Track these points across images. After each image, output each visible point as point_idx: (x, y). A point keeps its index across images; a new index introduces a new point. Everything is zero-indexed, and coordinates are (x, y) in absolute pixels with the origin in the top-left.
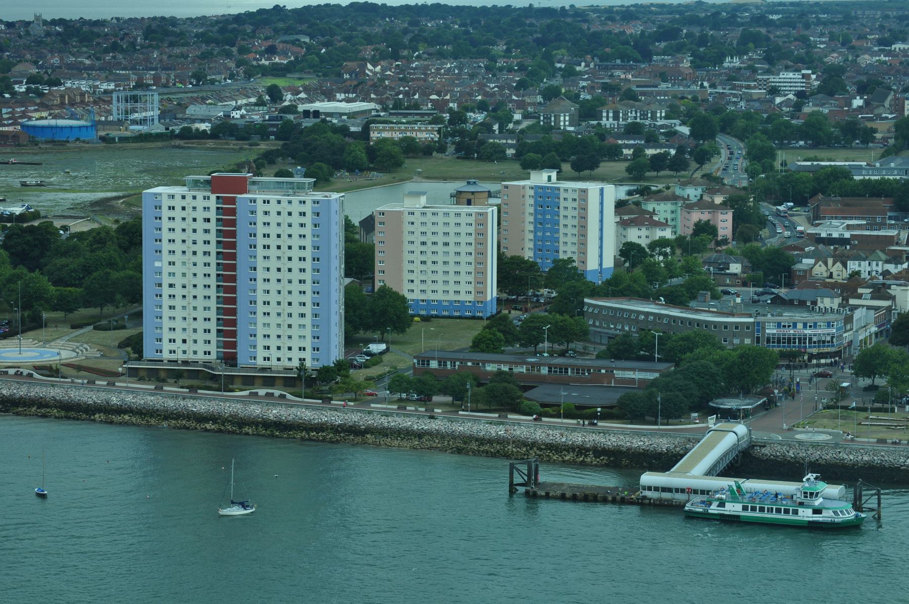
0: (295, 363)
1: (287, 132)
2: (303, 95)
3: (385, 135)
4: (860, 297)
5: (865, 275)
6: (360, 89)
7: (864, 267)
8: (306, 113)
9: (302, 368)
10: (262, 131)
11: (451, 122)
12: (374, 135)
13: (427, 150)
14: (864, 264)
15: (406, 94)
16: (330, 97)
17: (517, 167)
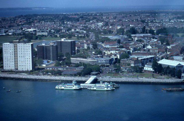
0: (27, 69)
1: (24, 34)
2: (26, 28)
3: (39, 34)
4: (112, 56)
5: (113, 53)
6: (35, 27)
7: (113, 52)
8: (27, 31)
9: (28, 70)
10: (20, 34)
11: (49, 32)
12: (37, 34)
13: (46, 36)
14: (113, 51)
15: (42, 28)
16: (30, 29)
17: (60, 38)
